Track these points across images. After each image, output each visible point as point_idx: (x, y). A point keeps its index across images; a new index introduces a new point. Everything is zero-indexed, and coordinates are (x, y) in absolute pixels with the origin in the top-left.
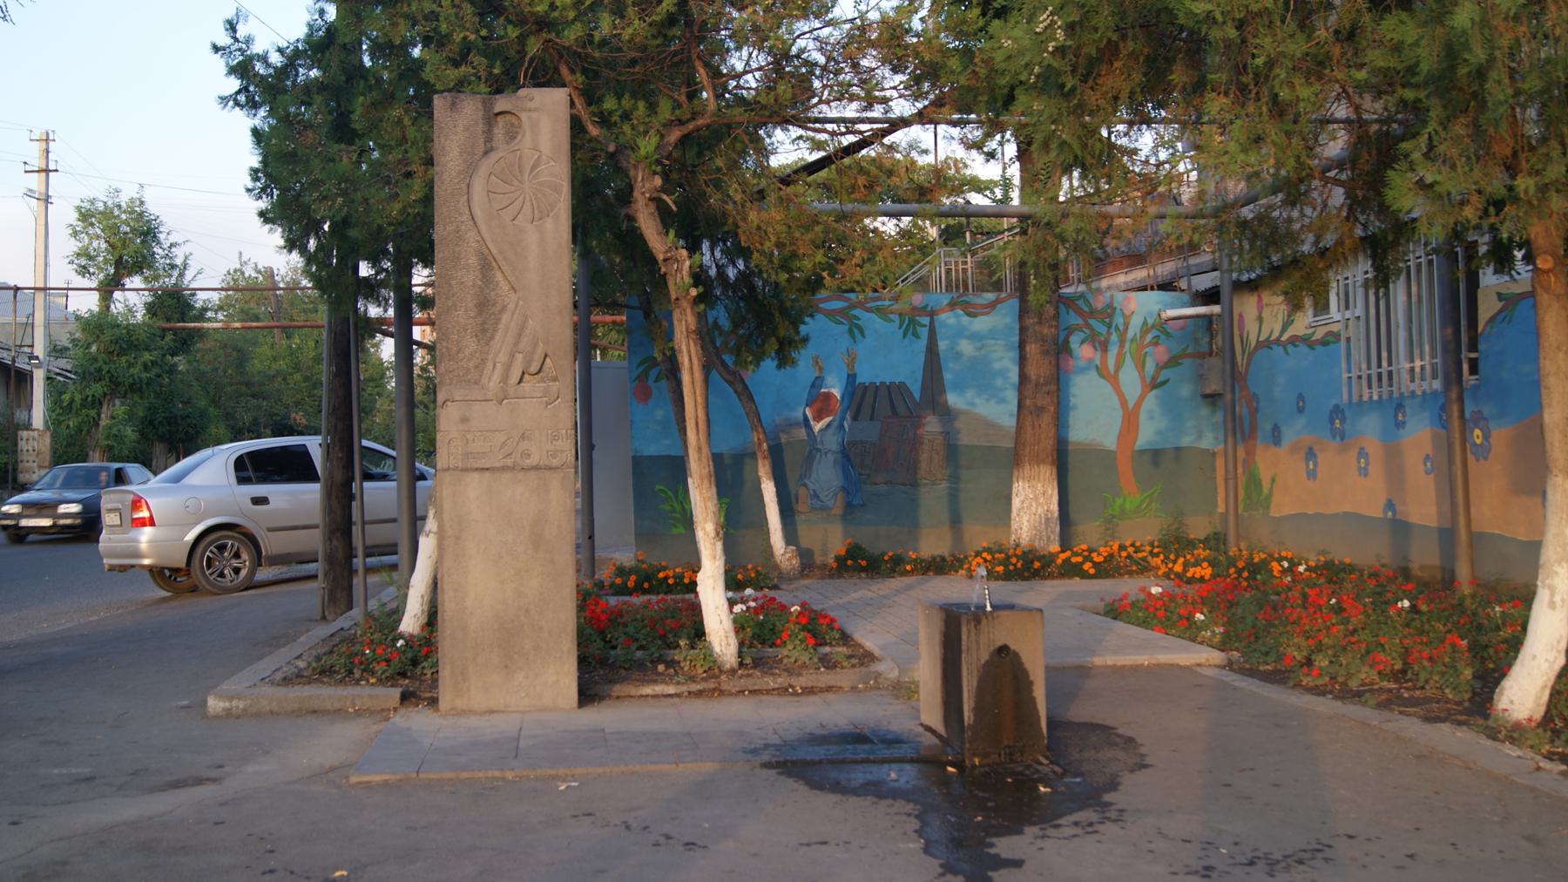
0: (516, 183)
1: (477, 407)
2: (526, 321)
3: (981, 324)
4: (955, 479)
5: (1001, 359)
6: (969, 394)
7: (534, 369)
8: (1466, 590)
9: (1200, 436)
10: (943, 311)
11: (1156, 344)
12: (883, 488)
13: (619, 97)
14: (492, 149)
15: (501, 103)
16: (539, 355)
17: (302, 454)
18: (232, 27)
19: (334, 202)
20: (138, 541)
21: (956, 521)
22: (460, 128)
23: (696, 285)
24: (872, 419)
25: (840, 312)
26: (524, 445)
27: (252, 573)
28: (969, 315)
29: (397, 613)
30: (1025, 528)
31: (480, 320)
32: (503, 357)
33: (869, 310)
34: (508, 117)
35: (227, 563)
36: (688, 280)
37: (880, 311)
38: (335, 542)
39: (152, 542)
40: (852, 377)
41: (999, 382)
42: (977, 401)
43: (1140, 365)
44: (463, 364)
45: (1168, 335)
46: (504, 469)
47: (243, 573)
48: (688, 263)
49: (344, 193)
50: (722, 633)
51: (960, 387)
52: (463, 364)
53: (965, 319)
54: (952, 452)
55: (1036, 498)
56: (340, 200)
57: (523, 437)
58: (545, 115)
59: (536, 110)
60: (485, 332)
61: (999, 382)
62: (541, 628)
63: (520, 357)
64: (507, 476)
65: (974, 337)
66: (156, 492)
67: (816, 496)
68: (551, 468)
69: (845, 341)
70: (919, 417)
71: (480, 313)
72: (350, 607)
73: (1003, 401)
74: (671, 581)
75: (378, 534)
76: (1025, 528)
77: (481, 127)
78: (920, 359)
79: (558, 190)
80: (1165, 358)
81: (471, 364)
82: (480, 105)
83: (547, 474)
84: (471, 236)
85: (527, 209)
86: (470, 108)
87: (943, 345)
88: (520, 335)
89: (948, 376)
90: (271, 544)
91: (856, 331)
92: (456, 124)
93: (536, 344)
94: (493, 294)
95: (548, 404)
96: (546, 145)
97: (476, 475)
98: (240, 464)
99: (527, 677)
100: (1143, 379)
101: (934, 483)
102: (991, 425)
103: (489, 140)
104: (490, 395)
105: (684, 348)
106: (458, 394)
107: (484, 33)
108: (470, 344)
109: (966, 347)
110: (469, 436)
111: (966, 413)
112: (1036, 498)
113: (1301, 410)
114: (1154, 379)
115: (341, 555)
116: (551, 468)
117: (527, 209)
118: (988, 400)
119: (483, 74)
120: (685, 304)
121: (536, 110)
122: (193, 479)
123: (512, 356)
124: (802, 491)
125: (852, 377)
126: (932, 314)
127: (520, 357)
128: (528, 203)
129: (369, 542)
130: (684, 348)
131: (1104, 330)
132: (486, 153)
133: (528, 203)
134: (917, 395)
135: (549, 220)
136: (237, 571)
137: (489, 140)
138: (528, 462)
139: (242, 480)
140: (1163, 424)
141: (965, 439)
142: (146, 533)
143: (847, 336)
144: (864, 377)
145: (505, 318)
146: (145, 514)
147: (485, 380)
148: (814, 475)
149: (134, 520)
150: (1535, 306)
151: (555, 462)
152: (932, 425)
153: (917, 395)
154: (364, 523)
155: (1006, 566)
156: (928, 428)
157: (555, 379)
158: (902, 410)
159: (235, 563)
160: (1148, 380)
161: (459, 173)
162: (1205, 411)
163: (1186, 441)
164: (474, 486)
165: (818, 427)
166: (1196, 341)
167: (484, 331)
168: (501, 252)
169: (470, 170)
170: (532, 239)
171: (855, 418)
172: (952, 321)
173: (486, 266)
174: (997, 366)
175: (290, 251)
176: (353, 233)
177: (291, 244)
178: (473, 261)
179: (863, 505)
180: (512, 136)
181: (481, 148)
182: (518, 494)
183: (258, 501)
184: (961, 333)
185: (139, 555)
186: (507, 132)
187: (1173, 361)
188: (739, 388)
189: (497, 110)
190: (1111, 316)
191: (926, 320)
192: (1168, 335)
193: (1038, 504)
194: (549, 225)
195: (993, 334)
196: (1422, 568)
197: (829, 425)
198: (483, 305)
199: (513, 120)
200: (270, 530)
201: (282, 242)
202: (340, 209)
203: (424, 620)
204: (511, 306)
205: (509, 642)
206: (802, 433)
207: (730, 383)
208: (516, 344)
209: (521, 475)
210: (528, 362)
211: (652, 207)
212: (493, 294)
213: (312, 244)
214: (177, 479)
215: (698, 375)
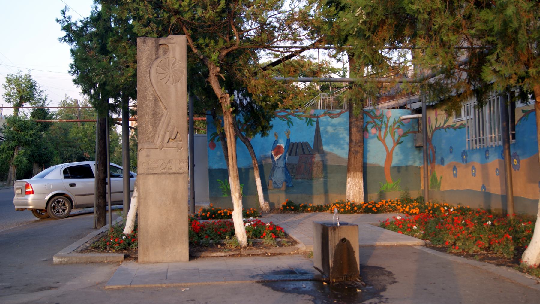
0: (167, 70)
1: (152, 151)
2: (170, 120)
3: (335, 121)
4: (326, 177)
5: (343, 134)
6: (331, 146)
7: (173, 137)
8: (511, 217)
9: (415, 162)
10: (321, 116)
11: (399, 128)
12: (300, 180)
13: (204, 38)
14: (158, 57)
15: (162, 41)
16: (175, 132)
17: (88, 168)
18: (64, 13)
19: (101, 76)
20: (27, 200)
21: (326, 192)
22: (147, 50)
23: (232, 107)
24: (296, 155)
25: (285, 116)
26: (170, 165)
27: (70, 211)
28: (331, 117)
29: (123, 226)
30: (351, 195)
31: (153, 119)
32: (162, 133)
33: (295, 116)
34: (164, 46)
35: (60, 208)
36: (229, 105)
37: (299, 116)
38: (100, 200)
39: (33, 200)
40: (288, 140)
41: (342, 142)
42: (334, 149)
43: (393, 136)
44: (148, 135)
45: (402, 124)
46: (162, 174)
47: (66, 211)
48: (229, 99)
49: (104, 73)
50: (241, 233)
51: (328, 144)
52: (148, 135)
53: (330, 119)
54: (325, 167)
55: (355, 184)
56: (103, 76)
57: (169, 162)
58: (178, 45)
59: (174, 43)
60: (155, 124)
61: (342, 142)
62: (175, 232)
63: (168, 133)
64: (164, 176)
65: (333, 125)
66: (34, 182)
67: (275, 183)
68: (179, 173)
69: (286, 127)
70: (313, 154)
71: (154, 117)
72: (105, 224)
73: (343, 149)
74: (223, 214)
75: (116, 197)
76: (351, 195)
77: (154, 50)
78: (314, 133)
79: (182, 72)
80: (402, 133)
81: (150, 136)
82: (154, 41)
83: (178, 175)
84: (151, 89)
85: (171, 79)
86: (150, 43)
87: (321, 129)
88: (168, 125)
89: (323, 140)
90: (77, 201)
91: (290, 123)
92: (145, 48)
93: (174, 128)
94: (158, 110)
95: (178, 150)
96: (178, 56)
97: (152, 176)
98: (65, 171)
99: (170, 250)
100: (394, 141)
102: (338, 157)
104: (157, 147)
105: (228, 130)
106: (145, 147)
107: (155, 15)
108: (150, 128)
109: (330, 129)
111: (330, 153)
112: (355, 184)
113: (451, 152)
114: (398, 141)
115: (102, 205)
116: (179, 173)
117: (171, 79)
118: (338, 149)
119: (155, 30)
120: (228, 114)
121: (174, 43)
122: (48, 177)
123: (165, 133)
124: (270, 181)
125: (288, 140)
126: (318, 117)
127: (168, 133)
128: (171, 77)
129: (112, 200)
130: (228, 130)
131: (379, 123)
132: (156, 59)
133: (171, 77)
134: (312, 147)
135: (179, 83)
136: (64, 210)
138: (171, 171)
139: (66, 177)
140: (401, 157)
141: (329, 163)
142: (31, 197)
143: (287, 125)
144: (293, 140)
145: (163, 119)
146: (30, 190)
147: (155, 141)
148: (275, 176)
149: (26, 192)
150: (536, 114)
151: (181, 171)
152: (317, 158)
153: (312, 147)
154: (111, 193)
155: (344, 209)
156: (316, 159)
157: (181, 141)
158: (307, 152)
159: (63, 208)
160: (396, 141)
161: (146, 66)
162: (416, 153)
163: (410, 163)
164: (151, 180)
165: (276, 158)
166: (413, 127)
167: (155, 123)
168: (161, 95)
169: (150, 65)
170: (172, 90)
171: (290, 155)
172: (325, 120)
173: (156, 100)
174: (341, 136)
175: (84, 94)
176: (107, 88)
177: (85, 92)
178: (151, 98)
179: (293, 187)
180: (165, 53)
181: (154, 57)
182: (167, 183)
183: (72, 185)
184: (328, 124)
185: (28, 205)
186: (164, 51)
187: (405, 134)
188: (248, 144)
189: (160, 43)
190: (382, 118)
191: (315, 120)
192: (402, 124)
193: (356, 186)
194: (179, 84)
195: (340, 124)
196: (495, 209)
197: (280, 158)
199: (166, 47)
200: (76, 195)
201: (81, 91)
202: (103, 79)
203: (132, 228)
204: (165, 114)
205: (164, 237)
206: (270, 160)
207: (244, 142)
208: (167, 128)
209: (168, 176)
210: (171, 134)
211: (216, 79)
212: (158, 110)
213: (92, 92)
214: (42, 177)
215: (233, 139)
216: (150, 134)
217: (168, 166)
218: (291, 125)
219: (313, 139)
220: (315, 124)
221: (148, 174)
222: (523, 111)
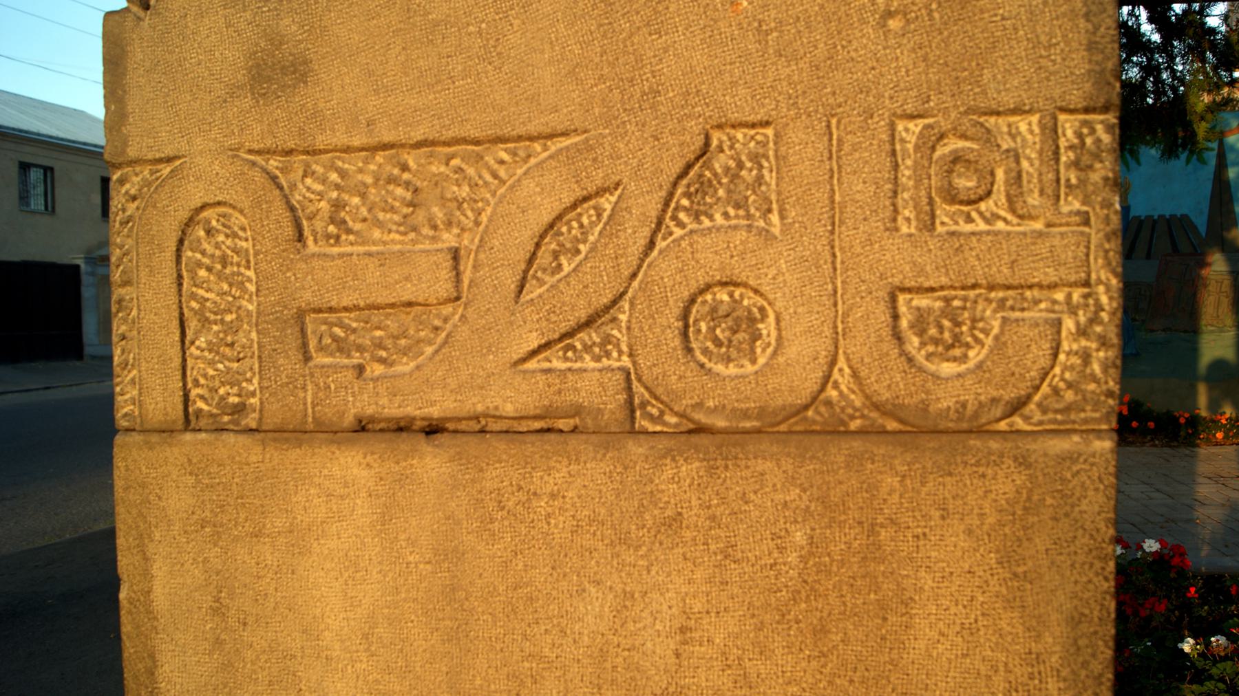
24: (1148, 256)
26: (710, 245)
46: (550, 427)
57: (694, 180)
64: (577, 482)
70: (1203, 254)
78: (1209, 186)
83: (891, 477)
101: (1221, 330)
110: (310, 191)
134: (1203, 230)
138: (733, 383)
151: (953, 381)
153: (1203, 230)
209: (680, 479)
217: (671, 275)
218: (1133, 164)
219: (1205, 206)
220: (1212, 158)
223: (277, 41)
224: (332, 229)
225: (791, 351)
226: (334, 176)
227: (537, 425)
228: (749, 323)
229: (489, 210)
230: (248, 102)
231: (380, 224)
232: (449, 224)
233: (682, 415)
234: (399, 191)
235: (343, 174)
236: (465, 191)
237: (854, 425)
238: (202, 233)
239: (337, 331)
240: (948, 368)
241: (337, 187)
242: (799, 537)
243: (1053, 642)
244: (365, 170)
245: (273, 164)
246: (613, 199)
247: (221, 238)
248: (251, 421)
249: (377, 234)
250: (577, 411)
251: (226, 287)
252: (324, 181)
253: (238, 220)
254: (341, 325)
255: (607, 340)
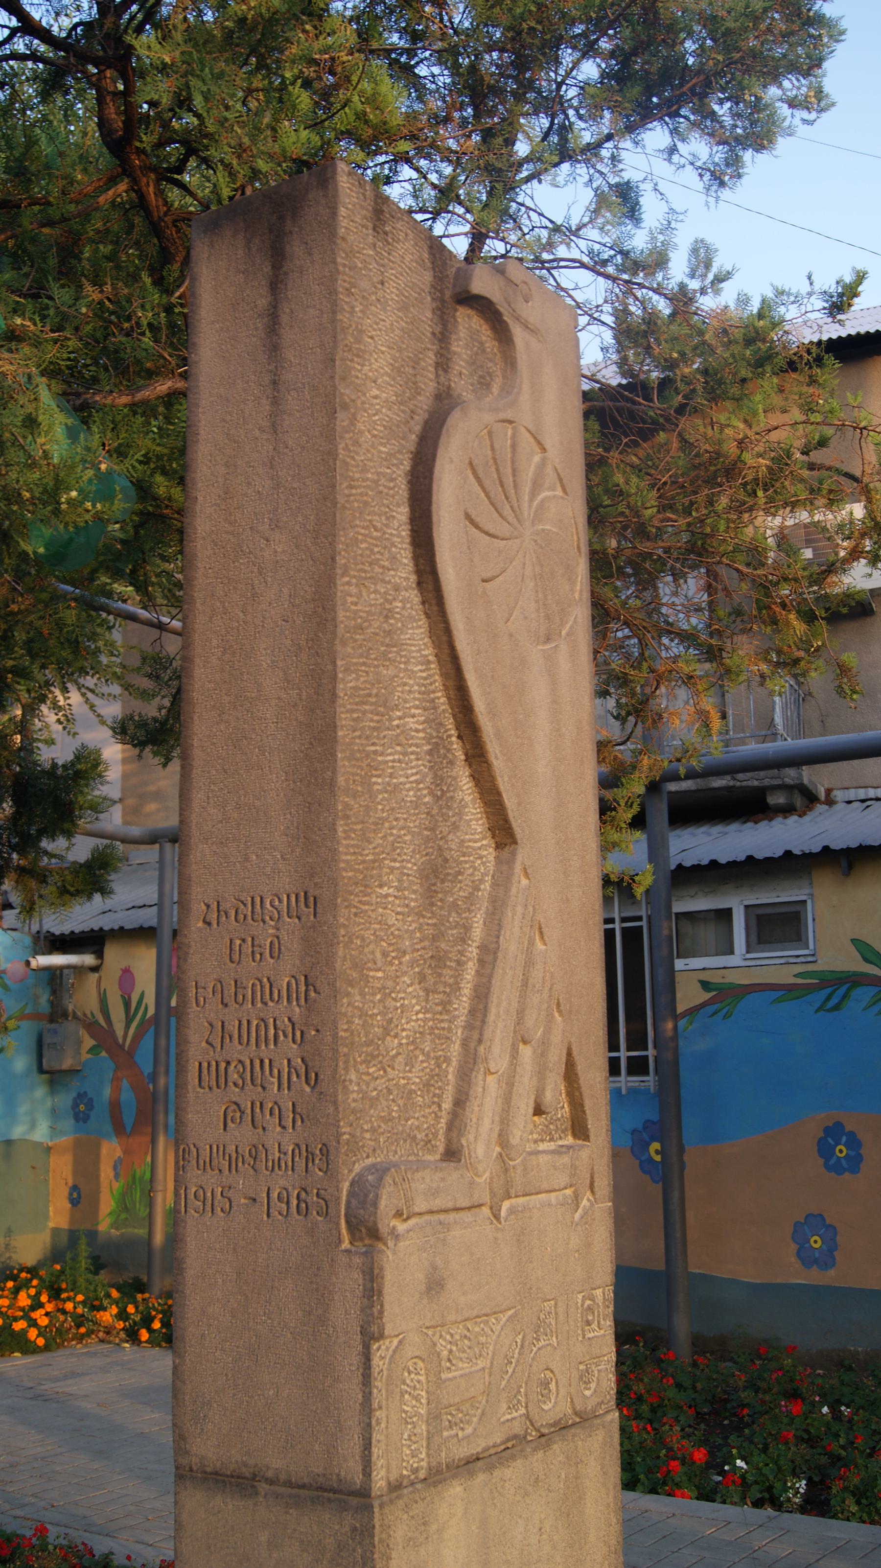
22: (391, 292)
63: (526, 1052)
64: (513, 1473)
81: (415, 1078)
97: (455, 1490)
103: (443, 364)
123: (515, 1054)
137: (443, 364)
167: (439, 960)
198: (437, 873)
216: (410, 1063)
221: (437, 1476)
222: (706, 985)
223: (435, 1268)
224: (448, 1364)
225: (561, 1394)
226: (448, 1337)
227: (503, 1447)
228: (546, 1384)
229: (491, 1348)
230: (425, 1301)
231: (461, 1359)
232: (480, 1355)
233: (538, 1430)
234: (466, 1341)
235: (452, 1335)
236: (483, 1339)
237: (570, 1422)
238: (406, 1374)
239: (449, 1417)
240: (587, 1393)
241: (450, 1343)
242: (563, 1476)
243: (611, 1499)
244: (458, 1331)
245: (430, 1333)
246: (520, 1337)
247: (413, 1376)
248: (422, 1474)
249: (460, 1365)
250: (515, 1437)
251: (414, 1402)
252: (445, 1340)
253: (421, 1364)
254: (451, 1414)
255: (519, 1401)
